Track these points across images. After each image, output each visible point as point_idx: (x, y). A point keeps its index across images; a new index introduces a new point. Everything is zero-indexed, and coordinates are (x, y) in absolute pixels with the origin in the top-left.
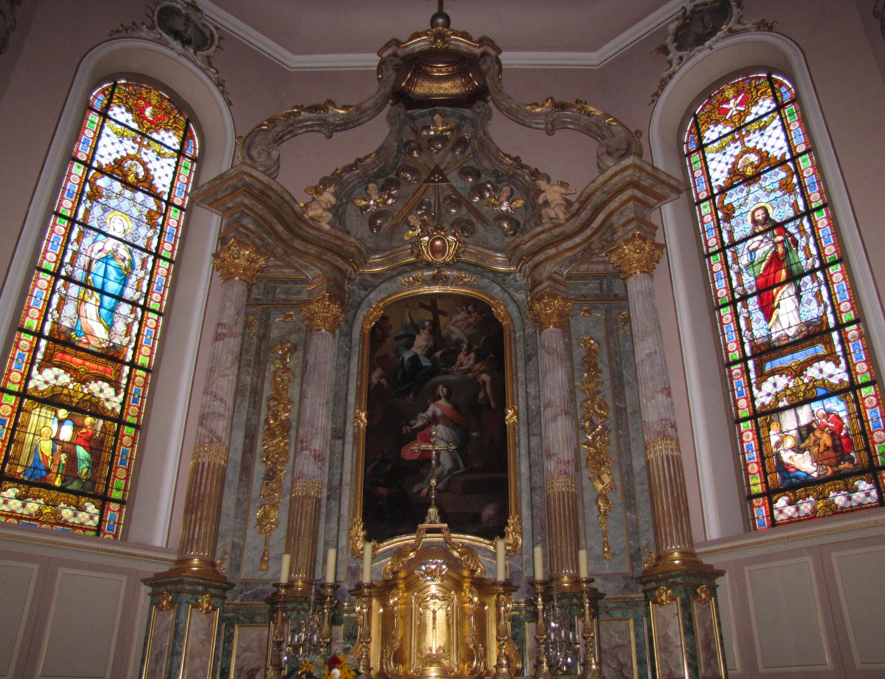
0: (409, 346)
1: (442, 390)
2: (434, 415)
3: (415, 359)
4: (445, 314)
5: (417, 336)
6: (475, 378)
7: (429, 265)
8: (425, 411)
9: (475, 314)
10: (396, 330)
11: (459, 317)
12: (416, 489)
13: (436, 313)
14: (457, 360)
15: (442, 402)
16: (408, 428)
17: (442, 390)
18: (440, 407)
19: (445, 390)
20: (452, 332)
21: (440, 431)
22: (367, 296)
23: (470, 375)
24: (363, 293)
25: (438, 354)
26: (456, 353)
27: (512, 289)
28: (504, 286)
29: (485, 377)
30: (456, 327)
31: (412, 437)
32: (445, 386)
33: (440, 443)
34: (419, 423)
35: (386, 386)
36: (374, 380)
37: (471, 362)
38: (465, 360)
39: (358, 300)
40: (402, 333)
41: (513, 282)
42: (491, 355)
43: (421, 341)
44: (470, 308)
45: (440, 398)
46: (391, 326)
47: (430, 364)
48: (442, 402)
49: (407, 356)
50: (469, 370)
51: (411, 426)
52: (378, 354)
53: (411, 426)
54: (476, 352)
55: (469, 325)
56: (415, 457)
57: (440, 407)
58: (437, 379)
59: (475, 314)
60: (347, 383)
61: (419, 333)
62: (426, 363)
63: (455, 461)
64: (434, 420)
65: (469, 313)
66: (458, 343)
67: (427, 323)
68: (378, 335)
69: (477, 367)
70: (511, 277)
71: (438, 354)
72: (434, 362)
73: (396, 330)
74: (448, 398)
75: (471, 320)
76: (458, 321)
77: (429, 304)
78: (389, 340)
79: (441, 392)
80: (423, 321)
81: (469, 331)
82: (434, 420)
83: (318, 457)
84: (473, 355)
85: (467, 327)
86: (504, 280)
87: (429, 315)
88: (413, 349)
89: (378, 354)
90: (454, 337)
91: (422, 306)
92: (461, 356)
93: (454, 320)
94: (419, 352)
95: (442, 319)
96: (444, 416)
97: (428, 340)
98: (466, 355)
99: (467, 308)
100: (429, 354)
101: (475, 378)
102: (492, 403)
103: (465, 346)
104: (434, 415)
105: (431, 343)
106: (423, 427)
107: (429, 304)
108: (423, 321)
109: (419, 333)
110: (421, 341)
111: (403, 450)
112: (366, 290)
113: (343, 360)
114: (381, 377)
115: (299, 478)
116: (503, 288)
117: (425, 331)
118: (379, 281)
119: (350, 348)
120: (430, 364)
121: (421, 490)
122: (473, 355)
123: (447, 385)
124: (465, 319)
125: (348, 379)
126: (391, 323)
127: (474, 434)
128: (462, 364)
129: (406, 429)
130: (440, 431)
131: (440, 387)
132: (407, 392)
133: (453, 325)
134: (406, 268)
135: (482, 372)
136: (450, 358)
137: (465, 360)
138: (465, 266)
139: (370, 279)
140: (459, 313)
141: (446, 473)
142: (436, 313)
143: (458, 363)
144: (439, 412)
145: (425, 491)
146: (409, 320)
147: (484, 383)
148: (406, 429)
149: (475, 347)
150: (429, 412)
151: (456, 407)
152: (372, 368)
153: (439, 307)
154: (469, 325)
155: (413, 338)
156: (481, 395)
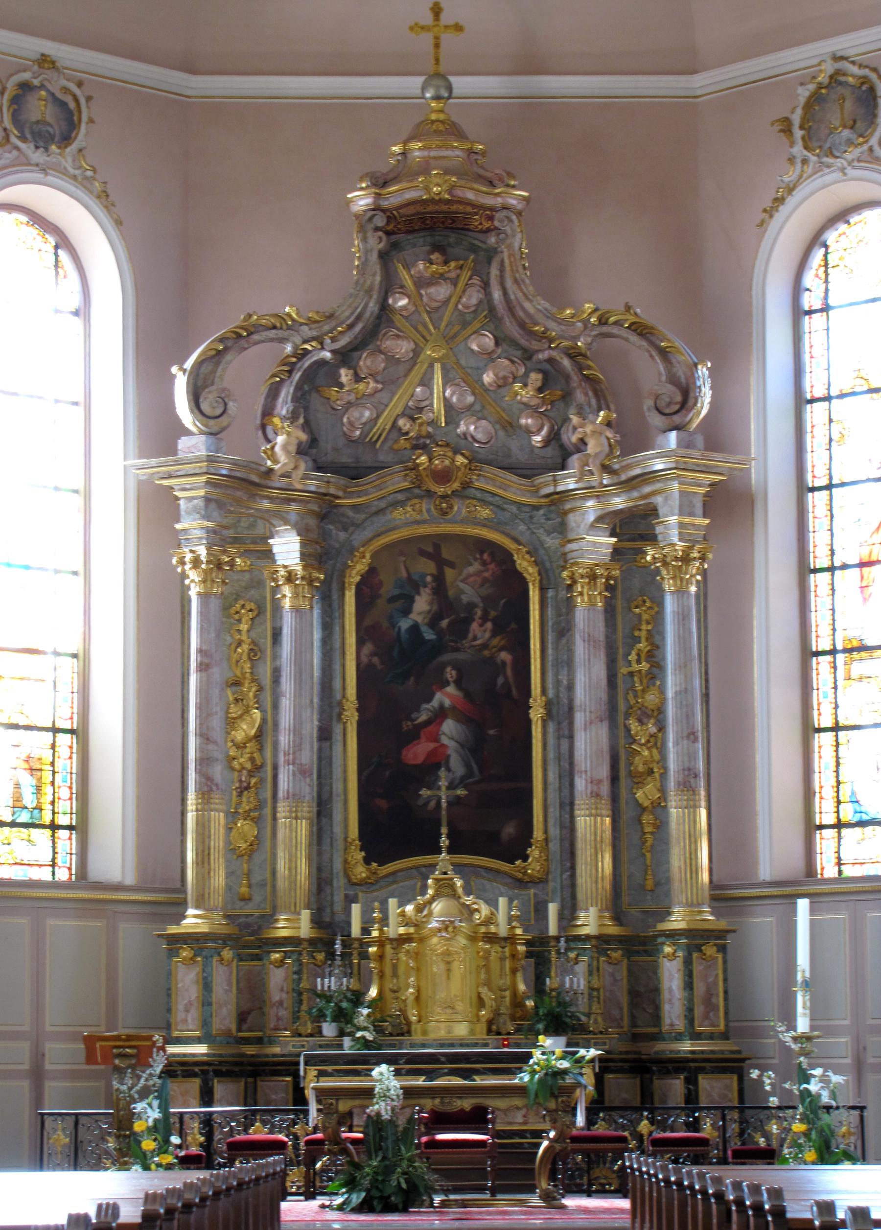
1: (450, 674)
2: (442, 706)
3: (415, 629)
4: (452, 565)
5: (417, 598)
9: (492, 566)
11: (471, 570)
13: (441, 563)
14: (467, 631)
15: (451, 689)
16: (409, 723)
17: (450, 674)
18: (448, 695)
19: (454, 673)
20: (462, 592)
21: (449, 727)
23: (486, 653)
25: (444, 623)
26: (468, 621)
29: (505, 656)
30: (468, 583)
31: (414, 735)
32: (454, 668)
34: (423, 717)
35: (379, 667)
36: (364, 659)
37: (487, 635)
40: (396, 592)
42: (513, 626)
43: (422, 604)
45: (447, 683)
48: (451, 689)
49: (404, 624)
50: (485, 646)
51: (413, 720)
53: (413, 720)
54: (495, 621)
57: (448, 695)
58: (446, 657)
62: (429, 635)
63: (467, 765)
64: (441, 714)
65: (484, 563)
66: (471, 606)
67: (429, 579)
69: (496, 641)
71: (444, 623)
72: (440, 633)
74: (458, 683)
78: (381, 602)
79: (449, 676)
82: (441, 714)
84: (489, 625)
85: (482, 585)
89: (367, 622)
90: (465, 599)
91: (423, 553)
92: (475, 626)
94: (419, 619)
95: (449, 573)
96: (453, 708)
97: (431, 603)
100: (433, 623)
101: (492, 658)
102: (514, 692)
104: (442, 706)
105: (435, 607)
106: (428, 723)
107: (430, 549)
108: (423, 576)
110: (422, 604)
111: (404, 752)
117: (428, 590)
127: (492, 732)
128: (475, 638)
130: (449, 727)
131: (448, 669)
135: (501, 649)
136: (461, 627)
140: (471, 564)
142: (441, 563)
143: (471, 636)
144: (447, 703)
147: (504, 663)
148: (407, 725)
149: (493, 613)
150: (435, 703)
151: (468, 695)
153: (446, 554)
155: (411, 600)
156: (500, 681)
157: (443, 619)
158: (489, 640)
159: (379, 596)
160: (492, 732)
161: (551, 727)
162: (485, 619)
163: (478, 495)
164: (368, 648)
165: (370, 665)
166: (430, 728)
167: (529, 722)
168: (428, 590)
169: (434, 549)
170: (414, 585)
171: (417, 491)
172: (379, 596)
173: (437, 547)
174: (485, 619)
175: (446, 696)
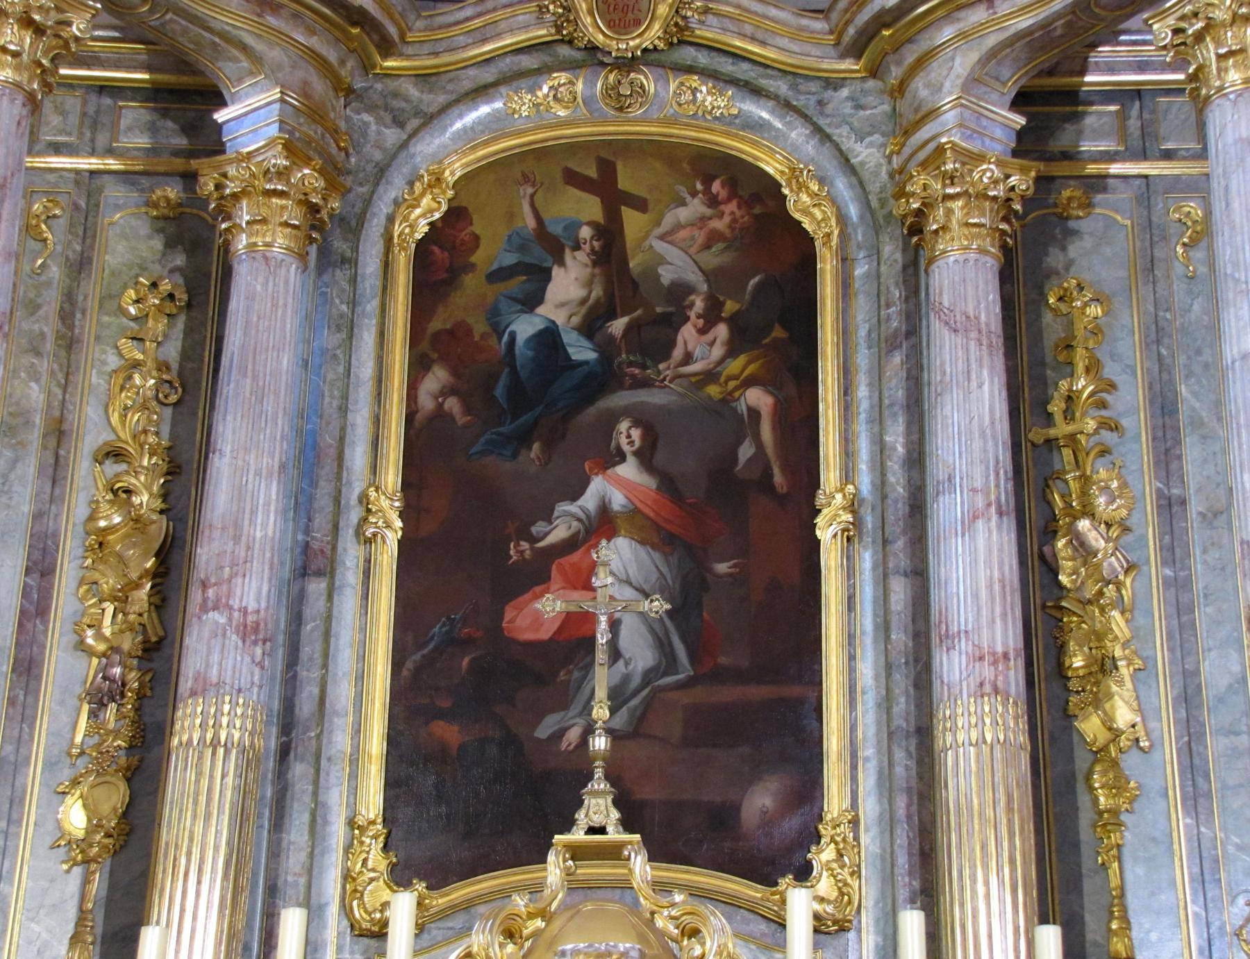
0: (532, 301)
1: (628, 435)
2: (604, 508)
3: (549, 338)
4: (641, 205)
5: (556, 272)
6: (727, 400)
7: (593, 56)
8: (575, 496)
9: (732, 207)
10: (492, 249)
11: (683, 214)
12: (544, 730)
13: (614, 200)
14: (672, 344)
15: (629, 470)
16: (525, 545)
17: (628, 435)
18: (621, 483)
19: (636, 434)
20: (662, 261)
21: (619, 556)
22: (404, 145)
23: (713, 390)
24: (392, 136)
25: (618, 326)
26: (673, 322)
27: (845, 130)
28: (822, 122)
29: (758, 398)
30: (674, 243)
31: (535, 575)
32: (636, 423)
33: (622, 588)
34: (559, 533)
35: (461, 419)
36: (426, 402)
37: (718, 352)
38: (700, 346)
39: (378, 156)
40: (510, 259)
41: (848, 109)
42: (778, 333)
43: (569, 286)
44: (716, 187)
45: (622, 457)
46: (476, 238)
47: (591, 355)
48: (629, 470)
49: (525, 328)
50: (710, 376)
51: (533, 540)
52: (435, 325)
53: (533, 540)
54: (734, 322)
55: (713, 238)
56: (545, 634)
57: (621, 483)
58: (621, 399)
59: (732, 207)
60: (343, 410)
61: (561, 263)
62: (581, 351)
63: (663, 645)
64: (603, 524)
65: (713, 202)
66: (680, 291)
67: (586, 232)
68: (440, 259)
69: (735, 366)
70: (845, 92)
71: (618, 326)
72: (607, 349)
73: (492, 249)
74: (645, 457)
75: (720, 225)
76: (679, 227)
77: (592, 172)
78: (472, 283)
79: (624, 441)
80: (573, 227)
81: (713, 259)
82: (603, 524)
83: (249, 632)
84: (722, 331)
85: (707, 246)
86: (821, 103)
87: (589, 208)
88: (541, 310)
89: (435, 325)
90: (667, 275)
91: (573, 179)
92: (687, 333)
93: (668, 221)
94: (560, 318)
95: (632, 221)
96: (634, 513)
97: (589, 284)
98: (702, 331)
99: (708, 182)
100: (591, 326)
101: (727, 400)
102: (778, 478)
103: (699, 304)
104: (604, 508)
105: (597, 292)
106: (570, 545)
107: (592, 172)
108: (573, 227)
109: (561, 263)
110: (569, 286)
111: (509, 614)
112: (399, 123)
113: (330, 339)
114: (446, 392)
115: (193, 694)
116: (818, 130)
117: (582, 256)
118: (441, 99)
119: (353, 303)
120: (591, 355)
121: (560, 734)
122: (722, 331)
123: (642, 419)
124: (703, 220)
125: (345, 397)
126: (477, 228)
127: (722, 568)
128: (688, 358)
129: (518, 551)
130: (619, 556)
131: (624, 426)
132: (523, 439)
133: (662, 238)
134: (527, 62)
135: (749, 383)
136: (655, 337)
137: (700, 346)
138: (703, 59)
139: (413, 92)
140: (683, 203)
141: (636, 682)
142: (614, 200)
143: (678, 353)
144: (618, 500)
145: (573, 735)
146: (531, 223)
147: (754, 413)
148: (518, 551)
149: (730, 306)
150: (589, 500)
151: (668, 484)
152: (419, 366)
153: (626, 181)
154: (713, 238)
155: (544, 276)
156: (746, 451)
157: (613, 316)
158: (721, 362)
159: (471, 267)
160: (722, 568)
161: (866, 560)
162: (711, 317)
163: (703, 59)
164: (436, 379)
165: (440, 414)
166: (575, 557)
167: (814, 545)
168: (582, 256)
169: (599, 170)
170: (552, 245)
171: (564, 51)
172: (471, 267)
173: (608, 169)
174: (711, 317)
175: (620, 485)
